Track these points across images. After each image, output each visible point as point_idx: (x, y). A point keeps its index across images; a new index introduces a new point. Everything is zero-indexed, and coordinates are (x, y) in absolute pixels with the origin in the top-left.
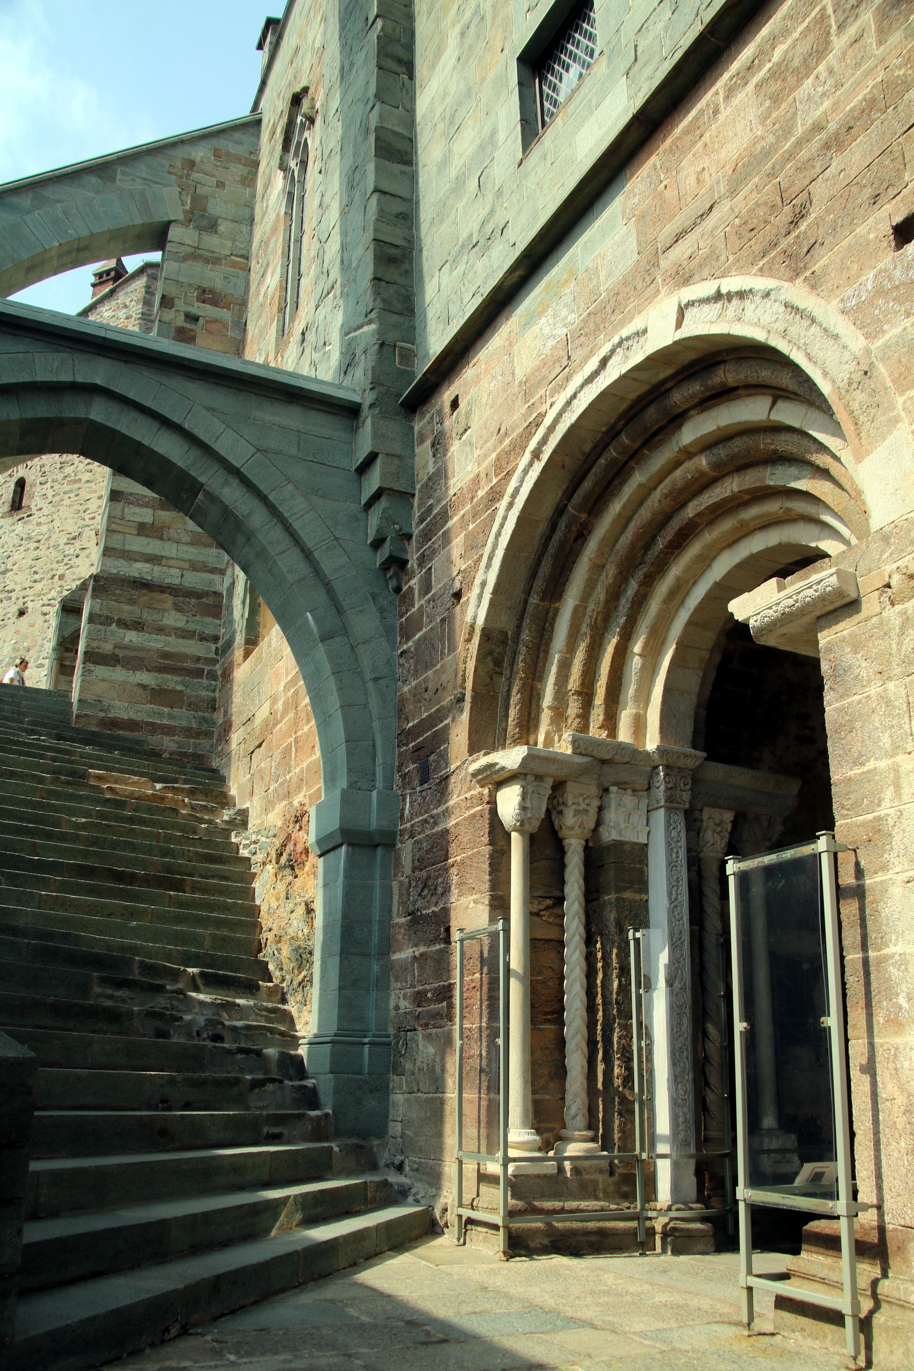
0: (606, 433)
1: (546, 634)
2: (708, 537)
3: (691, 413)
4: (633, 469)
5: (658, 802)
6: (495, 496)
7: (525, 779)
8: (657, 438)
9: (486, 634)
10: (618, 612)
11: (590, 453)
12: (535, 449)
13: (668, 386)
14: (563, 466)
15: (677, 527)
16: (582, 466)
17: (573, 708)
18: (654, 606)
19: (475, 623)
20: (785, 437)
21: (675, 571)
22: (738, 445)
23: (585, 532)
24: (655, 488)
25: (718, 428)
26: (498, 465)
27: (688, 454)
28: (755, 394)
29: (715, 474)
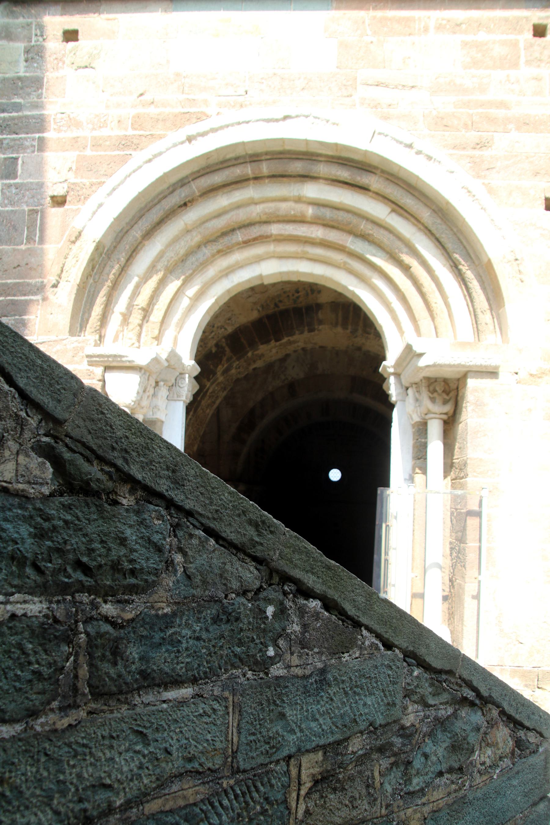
0: (251, 156)
1: (131, 259)
2: (271, 248)
3: (321, 181)
4: (248, 186)
5: (178, 396)
6: (128, 144)
7: (140, 371)
8: (281, 179)
9: (99, 247)
10: (184, 264)
11: (229, 160)
12: (193, 135)
13: (320, 159)
14: (208, 158)
15: (258, 234)
16: (217, 164)
17: (136, 318)
18: (211, 272)
19: (82, 231)
20: (382, 231)
21: (236, 257)
22: (341, 216)
23: (189, 204)
24: (256, 204)
25: (340, 203)
26: (138, 122)
27: (299, 200)
28: (378, 200)
29: (309, 219)
